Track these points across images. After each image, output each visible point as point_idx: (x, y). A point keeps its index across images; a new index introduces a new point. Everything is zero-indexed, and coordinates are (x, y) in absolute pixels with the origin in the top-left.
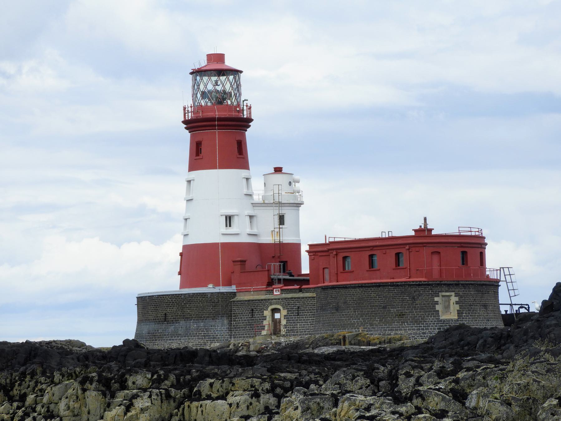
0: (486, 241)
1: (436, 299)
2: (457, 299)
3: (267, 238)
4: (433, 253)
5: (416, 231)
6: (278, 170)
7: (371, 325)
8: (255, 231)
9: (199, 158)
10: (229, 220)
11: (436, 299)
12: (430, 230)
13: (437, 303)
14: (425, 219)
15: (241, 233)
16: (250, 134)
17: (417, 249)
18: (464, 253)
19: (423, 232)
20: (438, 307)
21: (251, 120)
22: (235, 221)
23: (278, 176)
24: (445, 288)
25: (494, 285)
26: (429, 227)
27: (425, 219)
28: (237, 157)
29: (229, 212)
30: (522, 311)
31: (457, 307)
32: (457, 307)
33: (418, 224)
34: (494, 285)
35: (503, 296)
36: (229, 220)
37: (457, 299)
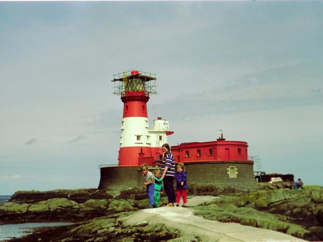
0: (248, 144)
1: (228, 169)
2: (237, 169)
3: (154, 145)
4: (226, 149)
5: (218, 140)
6: (159, 119)
7: (198, 180)
8: (149, 142)
9: (127, 113)
10: (138, 137)
11: (228, 169)
12: (225, 139)
13: (228, 171)
14: (222, 135)
15: (144, 143)
16: (148, 103)
17: (219, 147)
18: (239, 150)
19: (221, 140)
20: (228, 173)
21: (149, 98)
22: (141, 137)
23: (160, 121)
24: (231, 164)
25: (251, 163)
26: (224, 138)
27: (222, 135)
28: (143, 113)
29: (139, 134)
30: (262, 174)
31: (237, 173)
32: (237, 173)
33: (218, 136)
34: (251, 163)
35: (256, 168)
36: (138, 137)
37: (237, 169)
